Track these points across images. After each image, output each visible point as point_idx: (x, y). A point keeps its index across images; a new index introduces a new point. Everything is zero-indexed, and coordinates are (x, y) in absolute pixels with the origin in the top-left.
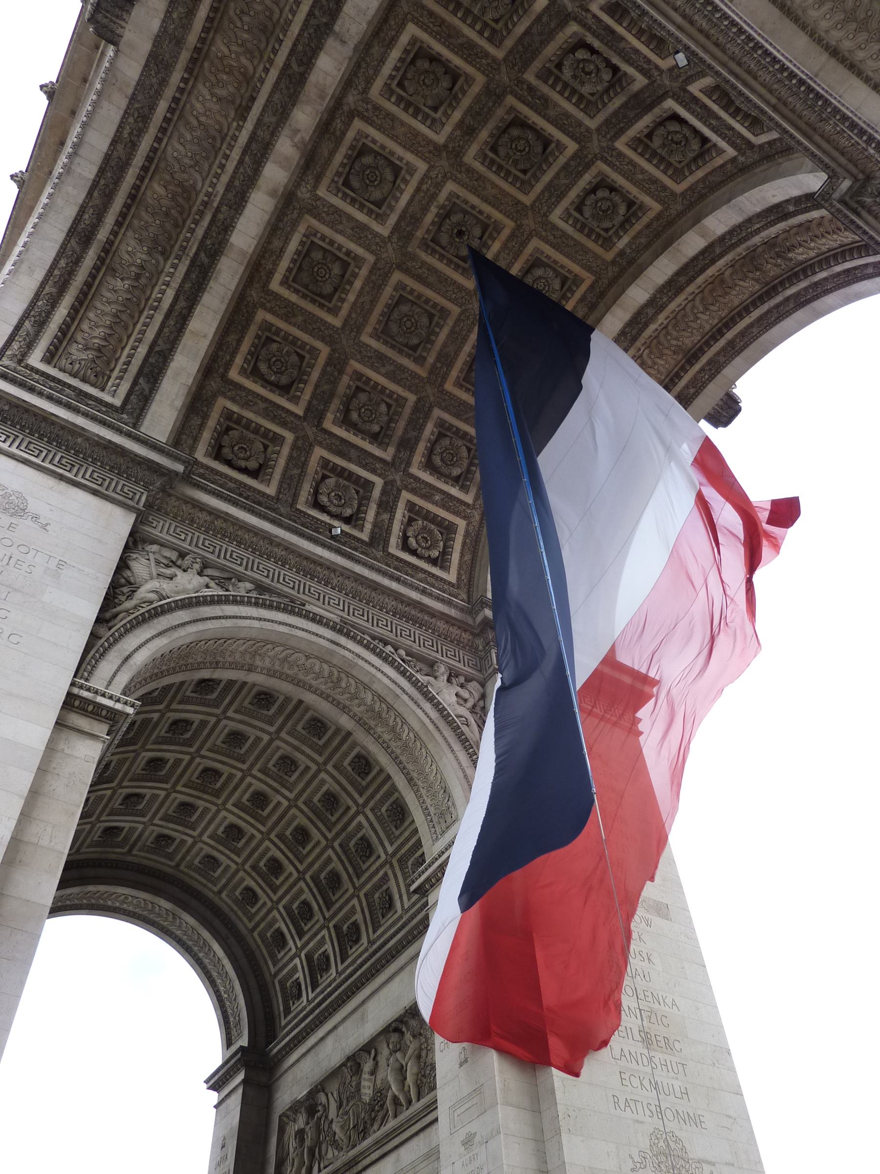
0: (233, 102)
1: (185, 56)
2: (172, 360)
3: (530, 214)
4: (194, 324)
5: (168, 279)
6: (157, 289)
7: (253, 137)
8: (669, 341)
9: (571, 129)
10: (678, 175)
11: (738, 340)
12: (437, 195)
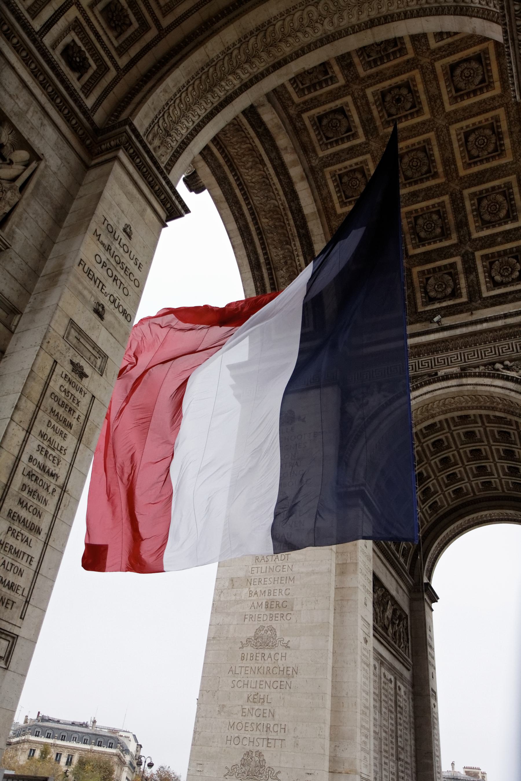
0: (257, 163)
1: (226, 168)
3: (420, 58)
5: (296, 253)
6: (297, 261)
7: (275, 168)
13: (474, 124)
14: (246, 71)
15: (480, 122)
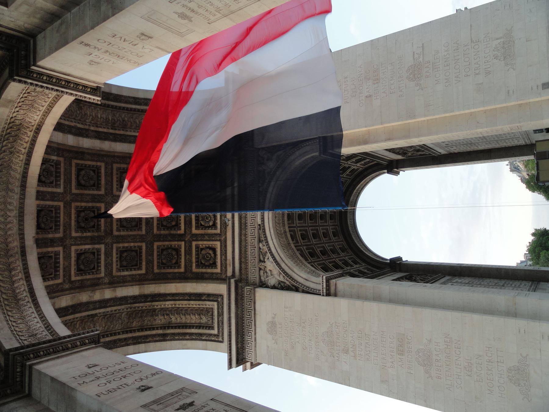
0: (93, 320)
3: (65, 200)
7: (100, 308)
8: (79, 114)
12: (79, 237)
13: (117, 181)
14: (17, 274)
15: (117, 178)
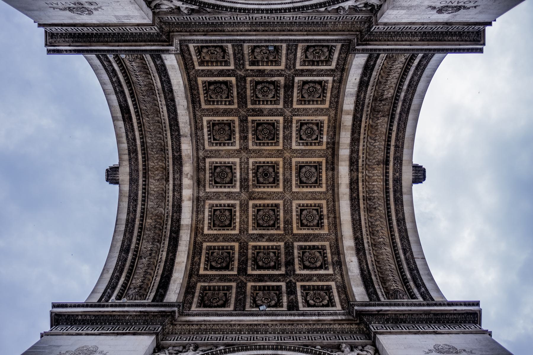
0: (163, 179)
2: (172, 277)
3: (285, 152)
4: (178, 260)
7: (174, 185)
9: (276, 113)
10: (323, 102)
11: (398, 143)
12: (248, 166)
